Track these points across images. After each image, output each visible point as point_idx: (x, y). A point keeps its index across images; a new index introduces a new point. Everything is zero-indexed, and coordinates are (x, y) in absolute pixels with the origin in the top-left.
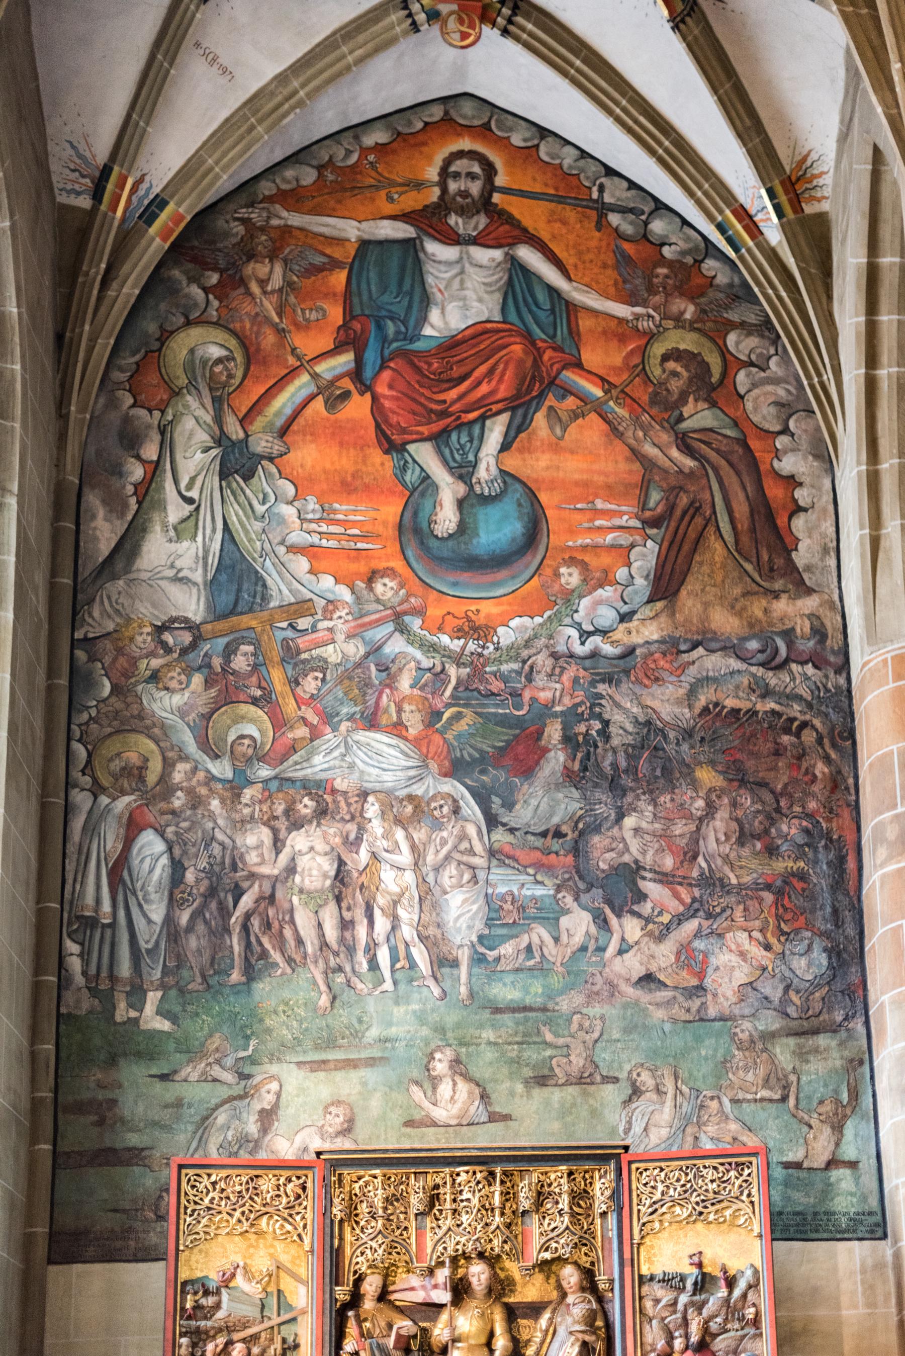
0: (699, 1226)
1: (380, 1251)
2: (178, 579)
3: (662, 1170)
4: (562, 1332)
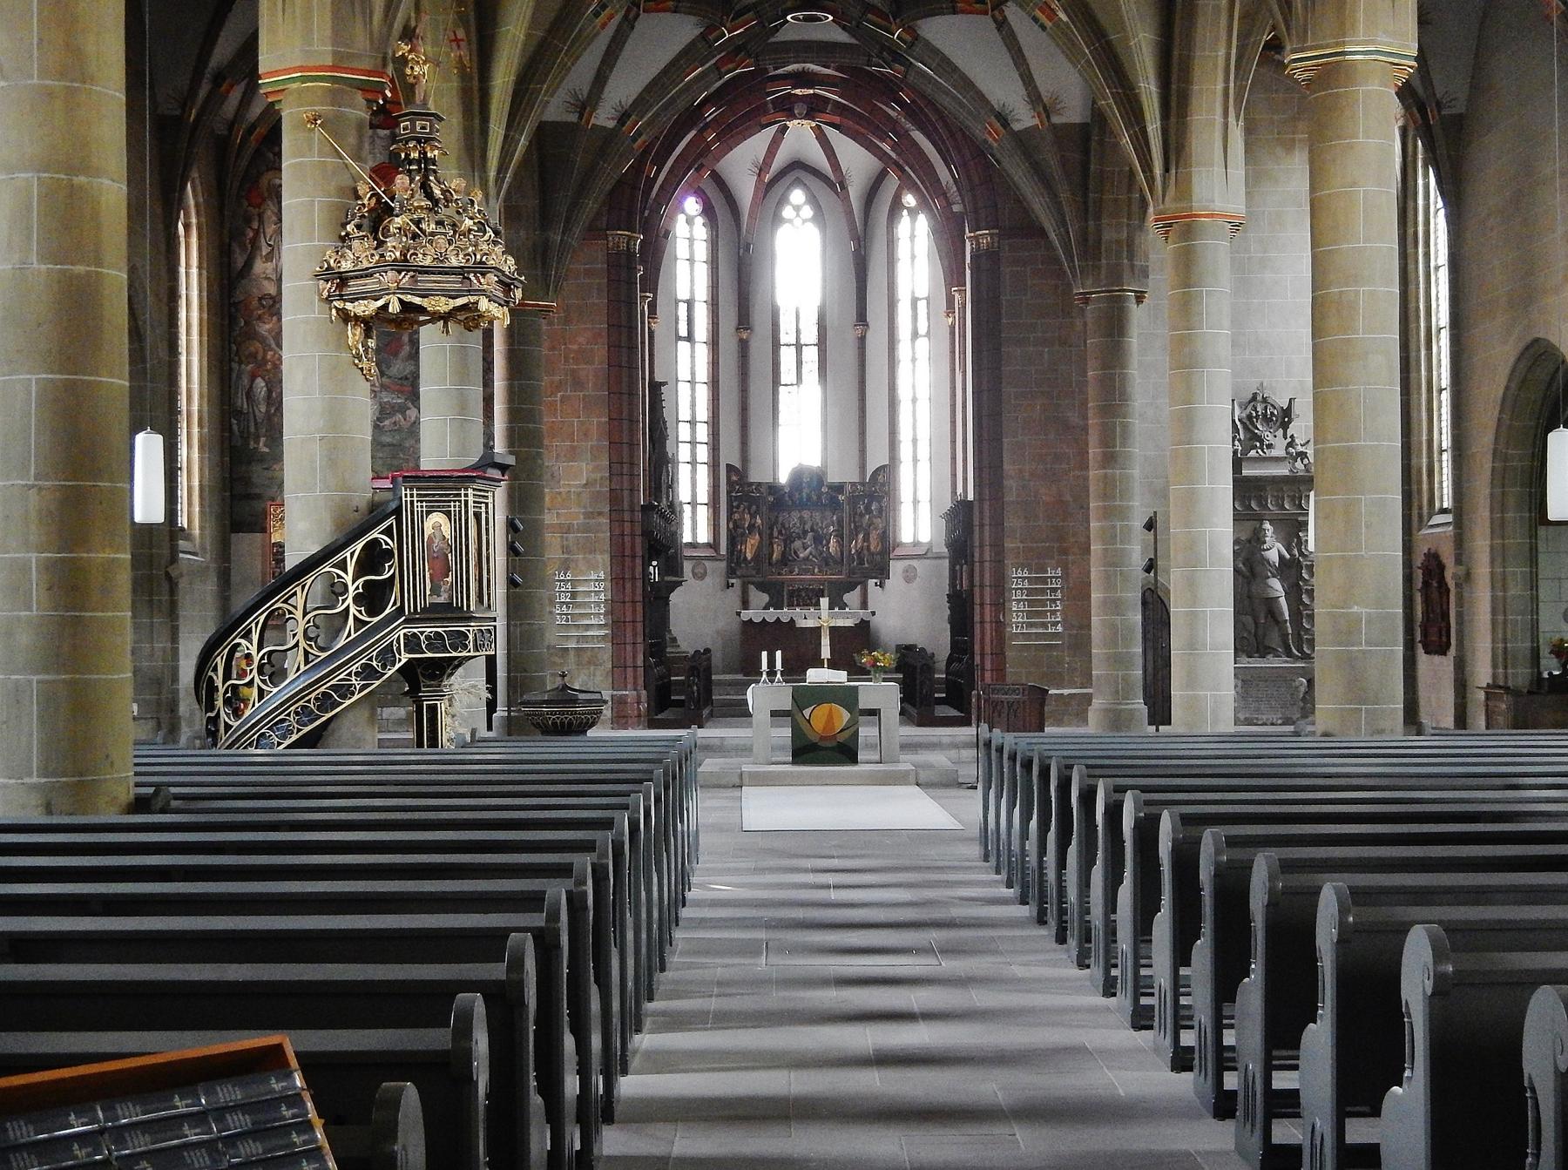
2: (267, 278)
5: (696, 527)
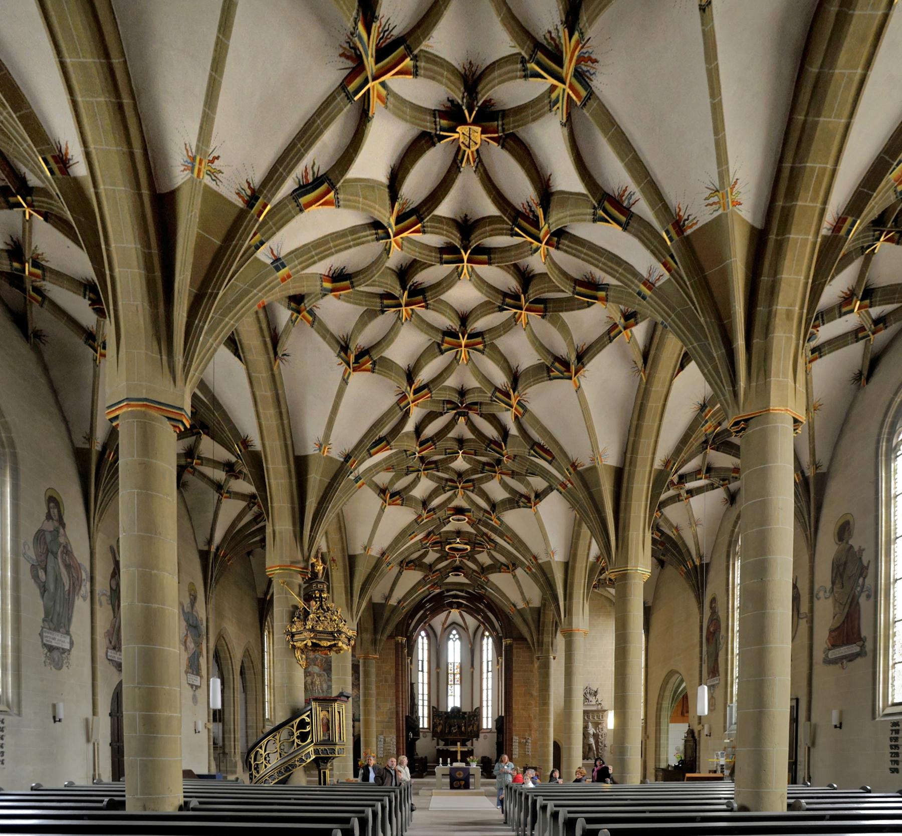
5: (424, 723)
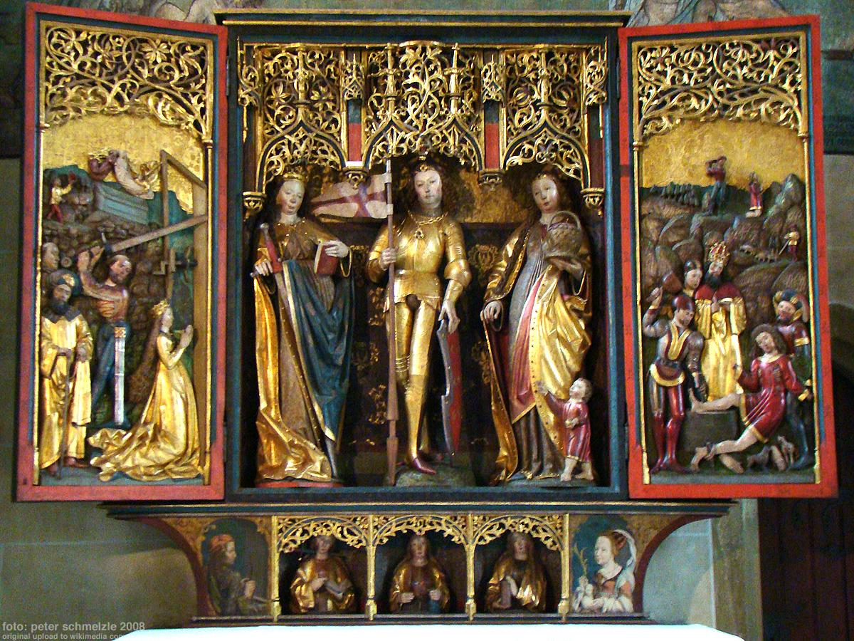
0: (721, 123)
1: (302, 148)
3: (673, 49)
4: (534, 259)
